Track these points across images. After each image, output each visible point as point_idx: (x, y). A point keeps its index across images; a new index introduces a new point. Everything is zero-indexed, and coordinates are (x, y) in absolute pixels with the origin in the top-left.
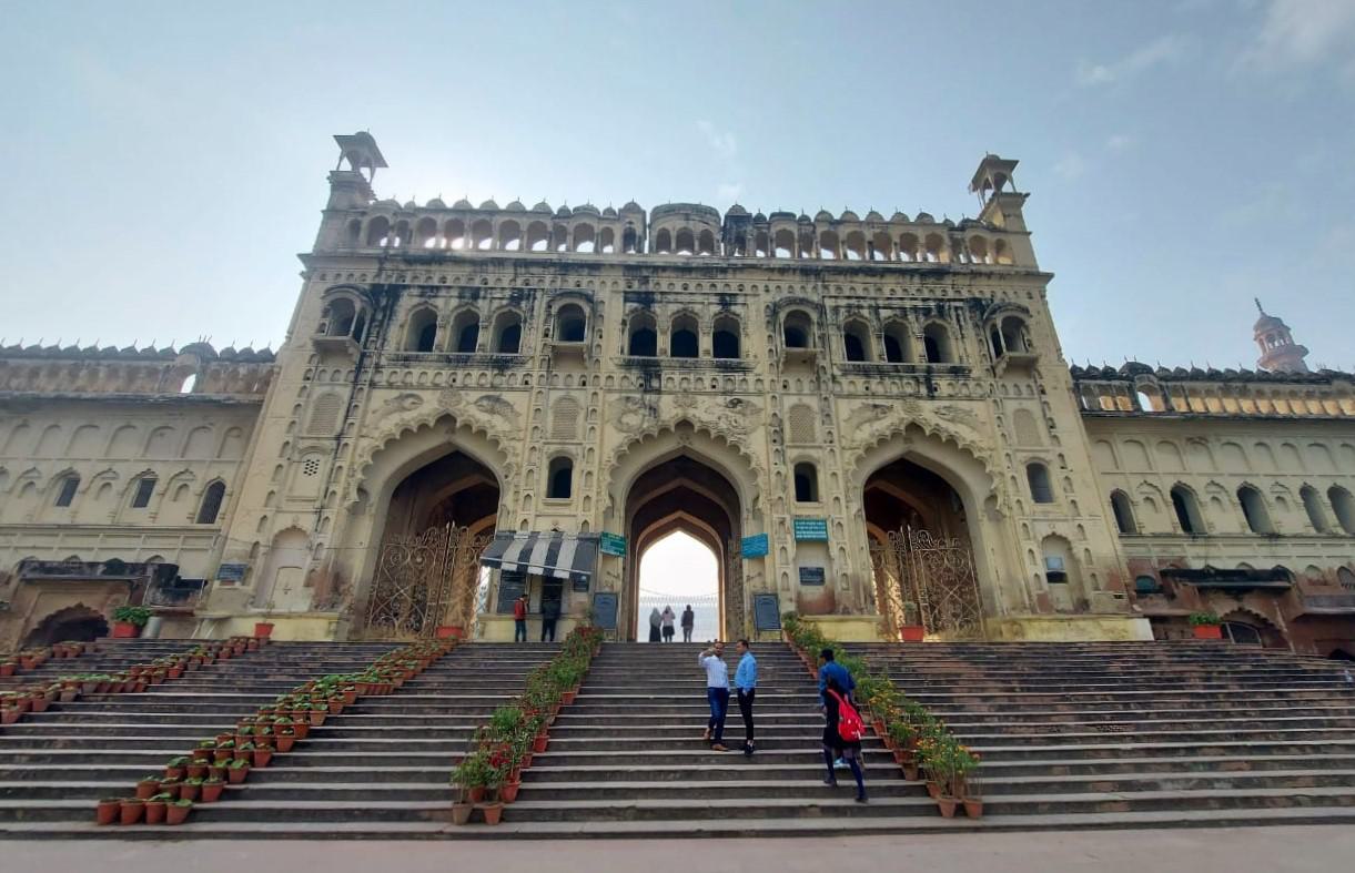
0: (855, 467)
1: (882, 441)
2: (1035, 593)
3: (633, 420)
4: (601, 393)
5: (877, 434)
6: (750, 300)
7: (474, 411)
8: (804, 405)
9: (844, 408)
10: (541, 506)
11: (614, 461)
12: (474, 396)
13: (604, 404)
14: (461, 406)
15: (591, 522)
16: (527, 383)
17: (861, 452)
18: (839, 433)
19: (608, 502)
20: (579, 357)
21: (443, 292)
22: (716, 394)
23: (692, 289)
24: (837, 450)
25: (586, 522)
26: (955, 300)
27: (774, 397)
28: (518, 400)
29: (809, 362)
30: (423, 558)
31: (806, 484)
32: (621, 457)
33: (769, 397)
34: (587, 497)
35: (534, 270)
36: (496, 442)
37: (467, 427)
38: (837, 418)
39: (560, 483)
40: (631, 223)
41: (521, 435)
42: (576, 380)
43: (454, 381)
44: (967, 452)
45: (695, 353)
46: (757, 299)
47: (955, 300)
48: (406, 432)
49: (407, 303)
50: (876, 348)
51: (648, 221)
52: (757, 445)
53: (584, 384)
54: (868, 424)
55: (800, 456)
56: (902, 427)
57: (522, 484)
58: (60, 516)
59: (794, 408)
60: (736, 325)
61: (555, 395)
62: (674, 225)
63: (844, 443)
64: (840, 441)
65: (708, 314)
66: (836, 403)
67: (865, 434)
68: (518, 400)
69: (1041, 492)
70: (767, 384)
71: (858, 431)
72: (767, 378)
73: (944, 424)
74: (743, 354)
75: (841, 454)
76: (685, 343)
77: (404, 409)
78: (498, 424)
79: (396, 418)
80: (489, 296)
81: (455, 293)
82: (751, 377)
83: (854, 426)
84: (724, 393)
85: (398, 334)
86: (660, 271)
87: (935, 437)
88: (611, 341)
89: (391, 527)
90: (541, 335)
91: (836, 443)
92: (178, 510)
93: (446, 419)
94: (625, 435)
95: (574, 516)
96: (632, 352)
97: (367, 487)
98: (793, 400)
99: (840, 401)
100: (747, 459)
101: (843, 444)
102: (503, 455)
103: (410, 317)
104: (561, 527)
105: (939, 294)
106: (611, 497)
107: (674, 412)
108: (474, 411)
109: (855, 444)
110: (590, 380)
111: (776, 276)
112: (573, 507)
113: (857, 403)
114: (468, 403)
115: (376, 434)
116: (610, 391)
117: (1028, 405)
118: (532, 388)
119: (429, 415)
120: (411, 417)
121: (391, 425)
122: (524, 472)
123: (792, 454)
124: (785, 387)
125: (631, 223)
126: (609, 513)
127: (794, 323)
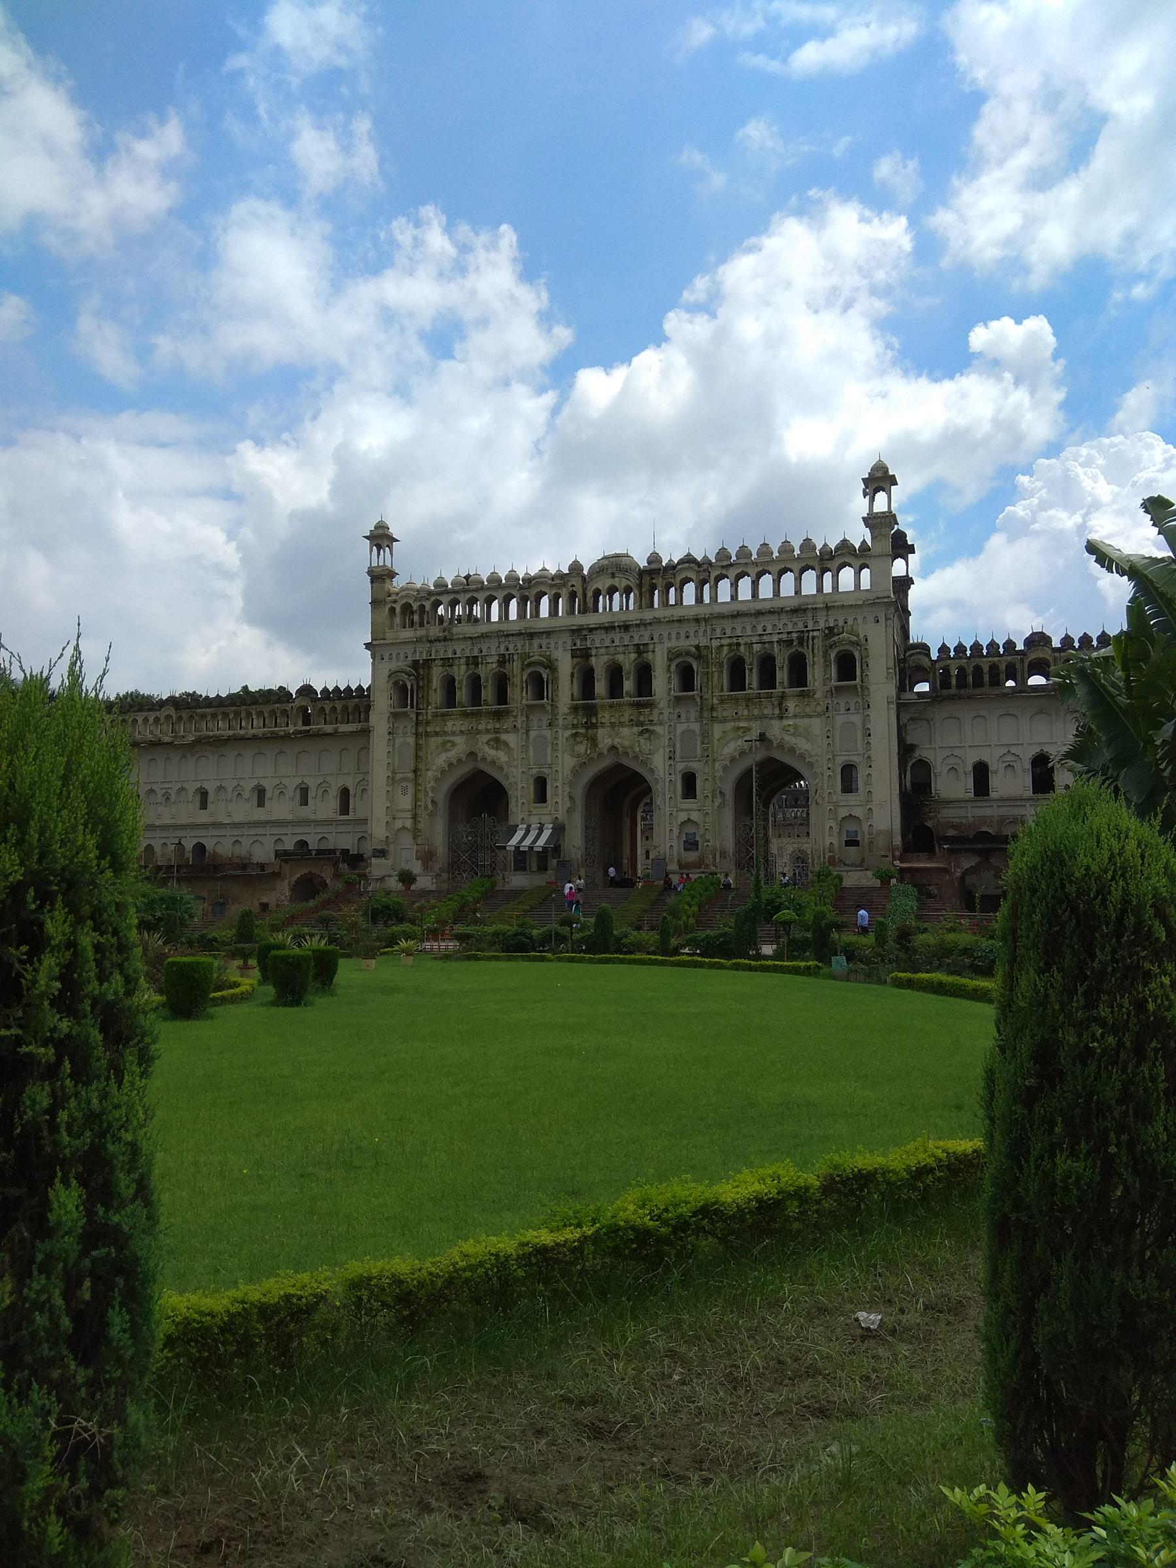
1: (742, 753)
2: (828, 854)
21: (456, 661)
28: (511, 739)
35: (510, 638)
42: (545, 723)
44: (802, 757)
48: (451, 765)
49: (437, 673)
50: (752, 678)
52: (659, 761)
58: (260, 814)
65: (628, 661)
68: (511, 739)
69: (848, 786)
72: (666, 712)
77: (447, 750)
79: (443, 757)
81: (463, 661)
82: (656, 712)
83: (729, 745)
85: (436, 696)
89: (452, 819)
92: (327, 808)
93: (472, 754)
100: (652, 771)
105: (801, 627)
108: (486, 749)
111: (676, 625)
117: (857, 719)
120: (452, 754)
123: (681, 766)
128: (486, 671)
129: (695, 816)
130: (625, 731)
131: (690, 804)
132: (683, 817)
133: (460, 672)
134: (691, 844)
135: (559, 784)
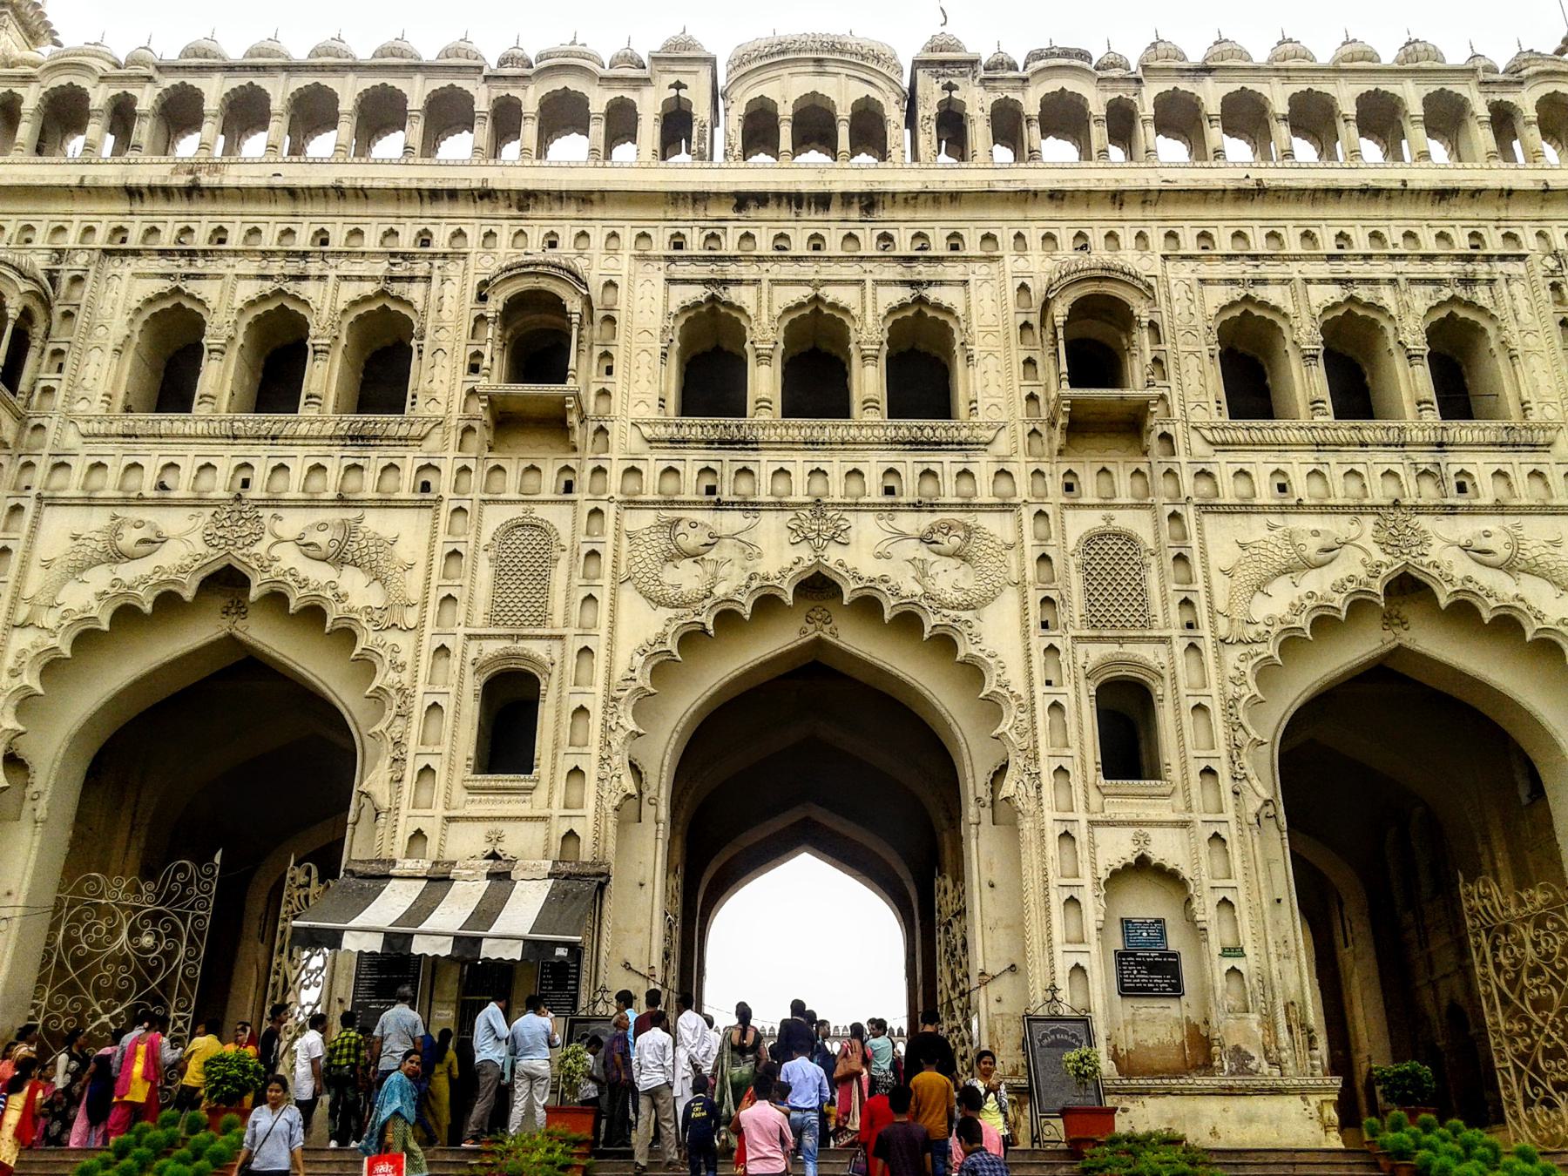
0: (1255, 690)
1: (1325, 623)
3: (686, 578)
4: (610, 511)
5: (1310, 603)
6: (981, 269)
7: (289, 558)
8: (1118, 535)
9: (1220, 541)
10: (459, 795)
11: (644, 681)
12: (293, 523)
13: (617, 538)
14: (260, 548)
15: (585, 829)
16: (426, 487)
17: (1270, 650)
18: (1211, 605)
19: (629, 784)
20: (553, 424)
22: (894, 508)
23: (833, 246)
24: (1207, 645)
25: (571, 834)
26: (1503, 258)
27: (1041, 513)
29: (1129, 426)
30: (158, 938)
31: (1127, 733)
32: (662, 669)
33: (1027, 514)
34: (576, 771)
36: (347, 635)
37: (276, 599)
38: (1206, 567)
39: (508, 724)
40: (678, 86)
41: (411, 618)
42: (549, 480)
43: (246, 484)
45: (839, 407)
46: (994, 265)
47: (1503, 258)
48: (126, 615)
51: (722, 82)
52: (999, 636)
53: (569, 487)
54: (1284, 581)
55: (1106, 664)
56: (1378, 587)
57: (412, 745)
59: (1093, 540)
60: (944, 333)
61: (496, 518)
62: (786, 92)
63: (1223, 628)
64: (1213, 623)
65: (870, 310)
66: (1200, 529)
67: (1280, 603)
70: (1023, 487)
71: (1259, 595)
72: (1021, 469)
73: (1487, 578)
74: (962, 407)
75: (1219, 657)
76: (816, 379)
78: (356, 592)
79: (100, 578)
80: (332, 273)
84: (917, 507)
86: (752, 204)
87: (1463, 612)
88: (634, 381)
89: (85, 850)
90: (462, 368)
91: (1205, 630)
93: (226, 583)
94: (671, 613)
95: (544, 819)
96: (688, 407)
97: (25, 750)
98: (1091, 521)
99: (1208, 520)
100: (973, 672)
101: (1222, 633)
102: (367, 666)
103: (138, 327)
104: (508, 848)
106: (635, 768)
107: (791, 554)
108: (289, 558)
109: (1251, 632)
110: (584, 479)
112: (541, 795)
113: (1255, 529)
114: (280, 540)
115: (50, 619)
116: (632, 504)
118: (440, 499)
119: (183, 570)
120: (139, 578)
121: (87, 597)
122: (418, 712)
124: (1069, 488)
125: (678, 86)
126: (630, 810)
127: (1095, 329)
128: (328, 303)
129: (1166, 849)
130: (866, 529)
131: (1130, 801)
132: (1117, 848)
133: (227, 301)
134: (1149, 970)
135: (595, 705)
